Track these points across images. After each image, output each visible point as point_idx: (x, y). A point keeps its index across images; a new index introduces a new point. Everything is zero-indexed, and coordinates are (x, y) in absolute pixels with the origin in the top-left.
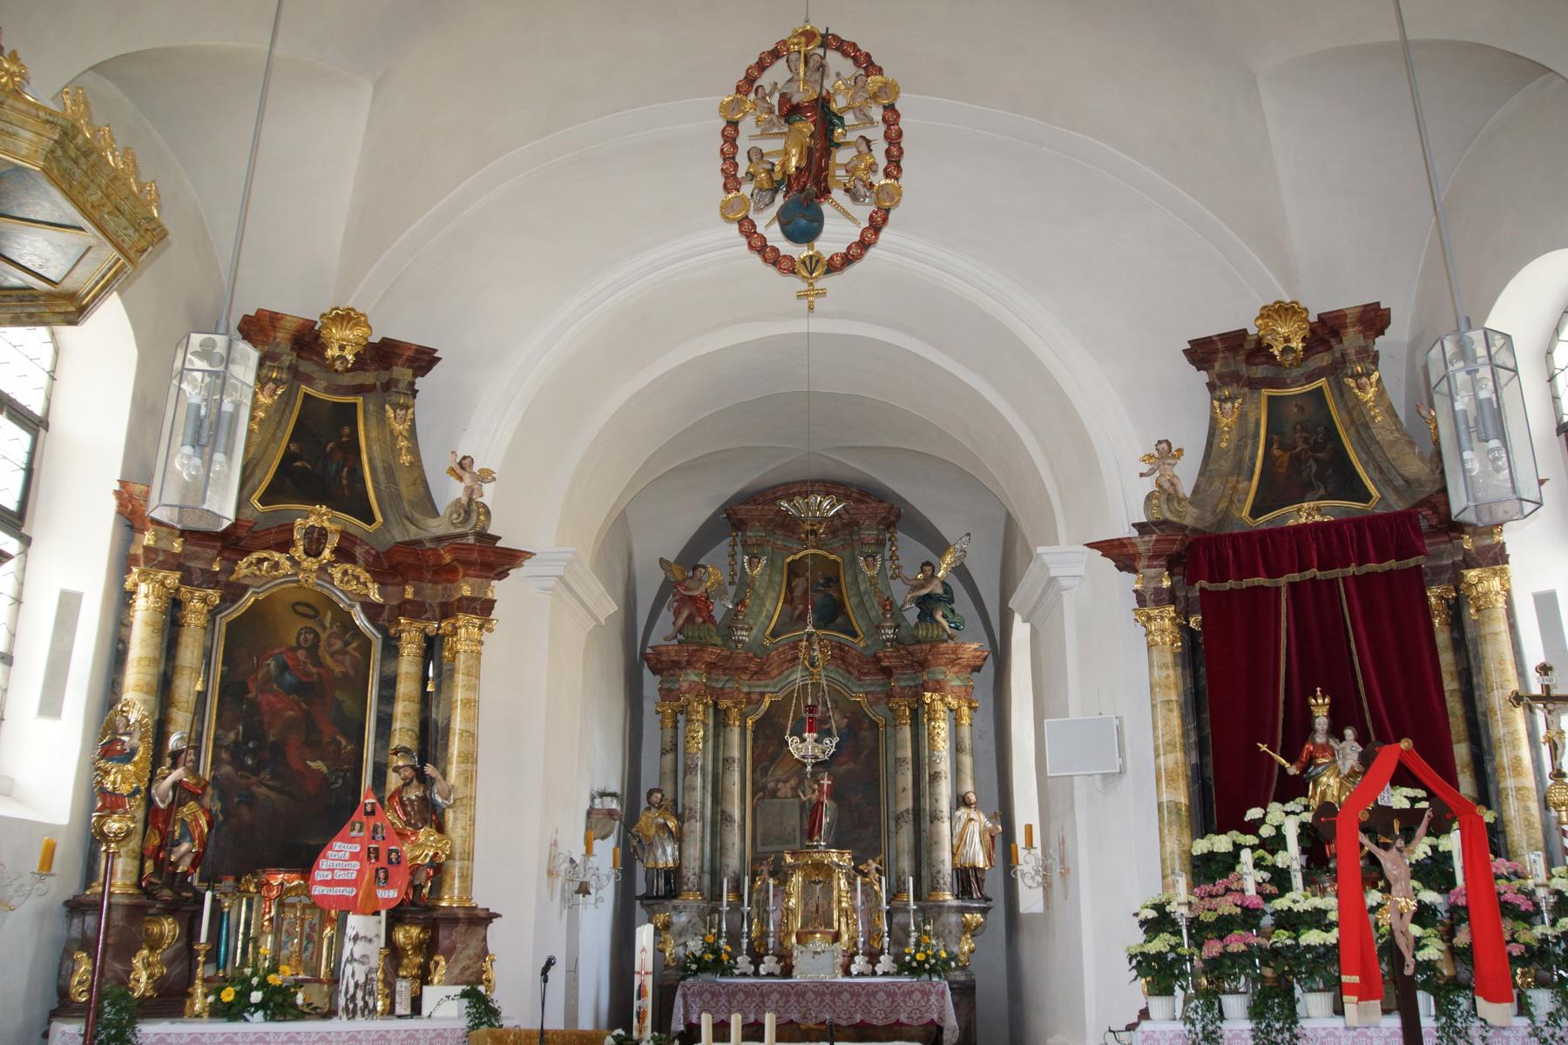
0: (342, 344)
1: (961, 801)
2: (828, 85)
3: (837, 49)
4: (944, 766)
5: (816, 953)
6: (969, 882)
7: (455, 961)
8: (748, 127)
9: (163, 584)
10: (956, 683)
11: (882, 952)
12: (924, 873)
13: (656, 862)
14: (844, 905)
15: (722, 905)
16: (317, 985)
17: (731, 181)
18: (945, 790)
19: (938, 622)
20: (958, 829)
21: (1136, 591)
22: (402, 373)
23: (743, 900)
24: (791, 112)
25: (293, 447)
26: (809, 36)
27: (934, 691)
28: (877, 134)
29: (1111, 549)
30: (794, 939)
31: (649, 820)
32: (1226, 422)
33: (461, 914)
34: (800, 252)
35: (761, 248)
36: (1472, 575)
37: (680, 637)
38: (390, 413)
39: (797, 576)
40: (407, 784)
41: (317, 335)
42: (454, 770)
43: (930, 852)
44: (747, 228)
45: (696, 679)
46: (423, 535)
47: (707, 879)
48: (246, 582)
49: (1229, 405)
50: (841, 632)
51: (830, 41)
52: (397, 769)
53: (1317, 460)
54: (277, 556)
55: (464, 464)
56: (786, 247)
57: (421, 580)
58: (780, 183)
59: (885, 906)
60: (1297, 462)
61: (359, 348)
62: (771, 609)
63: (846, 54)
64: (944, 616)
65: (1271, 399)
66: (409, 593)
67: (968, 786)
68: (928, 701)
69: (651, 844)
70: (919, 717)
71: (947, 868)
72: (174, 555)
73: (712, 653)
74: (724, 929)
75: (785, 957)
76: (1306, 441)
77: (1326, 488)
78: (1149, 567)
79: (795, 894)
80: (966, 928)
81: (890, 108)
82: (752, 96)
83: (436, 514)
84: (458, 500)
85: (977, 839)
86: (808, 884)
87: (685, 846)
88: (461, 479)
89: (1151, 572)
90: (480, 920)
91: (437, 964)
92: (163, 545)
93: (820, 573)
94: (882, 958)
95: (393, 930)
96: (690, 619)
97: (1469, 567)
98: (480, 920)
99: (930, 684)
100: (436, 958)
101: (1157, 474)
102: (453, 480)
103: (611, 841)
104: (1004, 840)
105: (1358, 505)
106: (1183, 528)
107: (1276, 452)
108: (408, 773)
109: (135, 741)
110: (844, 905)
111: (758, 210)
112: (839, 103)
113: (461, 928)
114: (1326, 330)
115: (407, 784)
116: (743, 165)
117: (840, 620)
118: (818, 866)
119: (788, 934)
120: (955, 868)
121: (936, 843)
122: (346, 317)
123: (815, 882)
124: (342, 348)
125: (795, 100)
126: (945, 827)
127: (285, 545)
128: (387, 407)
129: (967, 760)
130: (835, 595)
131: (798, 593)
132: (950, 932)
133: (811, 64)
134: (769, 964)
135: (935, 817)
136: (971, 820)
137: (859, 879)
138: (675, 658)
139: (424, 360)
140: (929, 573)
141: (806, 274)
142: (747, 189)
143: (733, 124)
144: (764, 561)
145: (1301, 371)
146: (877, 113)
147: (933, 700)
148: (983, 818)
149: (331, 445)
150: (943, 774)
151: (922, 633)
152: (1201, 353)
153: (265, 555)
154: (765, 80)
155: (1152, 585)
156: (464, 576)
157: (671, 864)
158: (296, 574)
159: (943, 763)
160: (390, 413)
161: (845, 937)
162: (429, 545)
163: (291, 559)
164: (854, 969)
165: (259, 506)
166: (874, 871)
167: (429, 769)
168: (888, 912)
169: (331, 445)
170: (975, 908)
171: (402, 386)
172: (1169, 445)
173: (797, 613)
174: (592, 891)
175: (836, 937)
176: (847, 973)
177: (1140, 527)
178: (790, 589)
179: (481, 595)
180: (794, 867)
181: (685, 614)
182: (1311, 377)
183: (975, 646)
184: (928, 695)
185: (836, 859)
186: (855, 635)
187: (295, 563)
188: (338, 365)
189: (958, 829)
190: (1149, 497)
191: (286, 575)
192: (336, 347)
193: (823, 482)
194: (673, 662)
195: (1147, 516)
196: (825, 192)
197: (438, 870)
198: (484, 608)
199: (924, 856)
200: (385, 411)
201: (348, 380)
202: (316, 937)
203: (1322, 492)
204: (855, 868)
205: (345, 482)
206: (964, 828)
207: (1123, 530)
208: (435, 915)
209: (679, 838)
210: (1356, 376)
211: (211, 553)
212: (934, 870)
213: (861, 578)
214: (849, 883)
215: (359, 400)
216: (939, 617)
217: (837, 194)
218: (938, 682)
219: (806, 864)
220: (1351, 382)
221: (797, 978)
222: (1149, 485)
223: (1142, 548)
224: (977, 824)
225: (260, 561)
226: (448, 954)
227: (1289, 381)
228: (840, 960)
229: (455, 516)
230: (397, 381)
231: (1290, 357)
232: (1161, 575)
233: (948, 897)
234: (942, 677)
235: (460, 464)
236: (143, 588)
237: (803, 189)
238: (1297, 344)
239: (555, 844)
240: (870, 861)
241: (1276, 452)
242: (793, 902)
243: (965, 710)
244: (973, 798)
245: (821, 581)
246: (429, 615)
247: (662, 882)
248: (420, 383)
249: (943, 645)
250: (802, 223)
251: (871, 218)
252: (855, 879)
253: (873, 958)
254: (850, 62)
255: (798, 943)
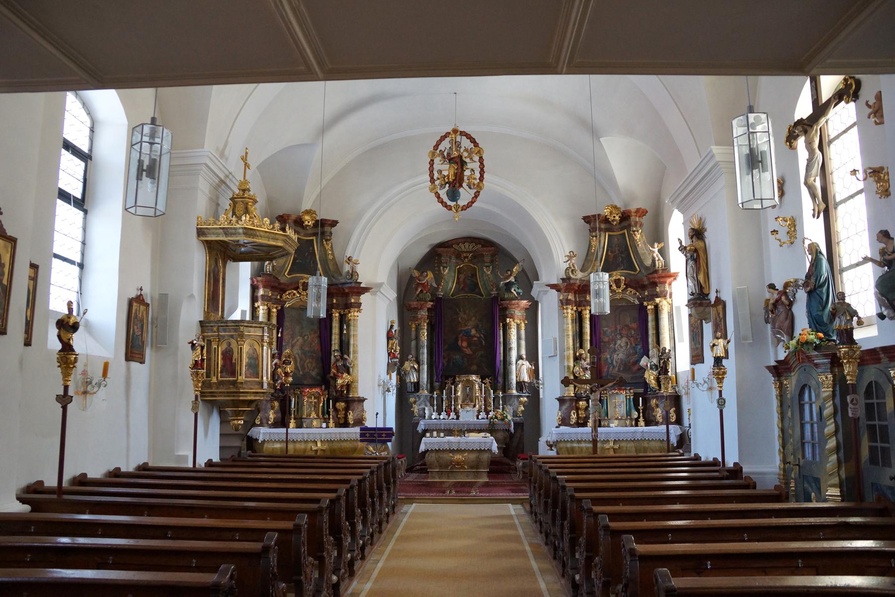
0: (308, 221)
1: (520, 357)
2: (462, 150)
3: (465, 136)
4: (514, 345)
5: (468, 411)
6: (523, 387)
7: (355, 412)
8: (437, 160)
9: (267, 306)
10: (520, 314)
11: (491, 411)
12: (506, 383)
13: (410, 379)
14: (477, 394)
15: (434, 394)
16: (319, 420)
17: (432, 180)
18: (514, 354)
19: (512, 292)
20: (519, 367)
21: (560, 300)
22: (327, 229)
23: (443, 394)
24: (451, 160)
25: (296, 256)
26: (455, 131)
27: (511, 318)
28: (476, 166)
29: (553, 286)
30: (460, 407)
31: (407, 365)
32: (593, 243)
33: (356, 399)
34: (452, 204)
35: (442, 202)
36: (658, 300)
37: (418, 298)
38: (325, 243)
39: (461, 273)
40: (337, 360)
41: (301, 219)
42: (351, 356)
43: (508, 376)
44: (438, 196)
45: (424, 314)
46: (337, 282)
47: (429, 385)
48: (286, 300)
49: (595, 238)
50: (477, 294)
51: (463, 134)
52: (335, 356)
53: (622, 257)
54: (295, 292)
55: (349, 259)
56: (449, 203)
57: (338, 297)
58: (447, 183)
59: (492, 396)
60: (615, 257)
61: (313, 222)
62: (451, 286)
63: (467, 138)
64: (515, 290)
65: (609, 235)
66: (335, 301)
67: (523, 352)
68: (508, 322)
69: (409, 373)
70: (506, 328)
71: (514, 382)
72: (270, 297)
73: (430, 304)
74: (435, 403)
75: (457, 413)
76: (619, 250)
77: (624, 267)
78: (565, 292)
79: (460, 391)
80: (521, 403)
81: (481, 160)
82: (438, 151)
83: (341, 274)
84: (348, 272)
85: (525, 371)
86: (464, 388)
87: (420, 375)
88: (349, 264)
89: (566, 294)
90: (362, 400)
91: (350, 413)
92: (266, 294)
93: (469, 272)
94: (490, 413)
95: (336, 404)
96: (421, 291)
97: (658, 297)
98: (362, 400)
99: (509, 315)
100: (350, 412)
101: (569, 262)
102: (347, 264)
103: (395, 373)
104: (535, 373)
105: (632, 273)
106: (576, 279)
107: (609, 253)
108: (339, 357)
109: (291, 360)
110: (477, 394)
111: (440, 189)
112: (465, 154)
113: (356, 403)
114: (625, 217)
115: (337, 360)
116: (436, 175)
117: (477, 290)
118: (468, 381)
119: (458, 405)
120: (517, 383)
121: (510, 373)
122: (308, 212)
123: (467, 387)
124: (309, 222)
125: (452, 156)
126: (514, 367)
127: (297, 288)
128: (324, 240)
129: (523, 343)
130: (475, 281)
131: (461, 280)
132: (515, 404)
133: (457, 144)
134: (453, 415)
135: (510, 364)
136: (523, 364)
137: (483, 385)
138: (416, 306)
139: (334, 223)
140: (509, 274)
141: (455, 211)
142: (437, 183)
143: (432, 160)
144: (448, 267)
145: (619, 227)
146: (476, 158)
147: (510, 321)
148: (528, 363)
149: (307, 254)
150: (513, 349)
151: (506, 296)
152: (587, 219)
153: (290, 292)
154: (441, 147)
155: (566, 298)
156: (352, 296)
157: (416, 381)
158: (300, 296)
159: (513, 344)
160: (325, 243)
161: (477, 406)
162: (340, 286)
163: (298, 292)
164: (480, 417)
165: (287, 276)
166: (488, 382)
167: (346, 356)
168: (494, 398)
169: (307, 254)
170: (524, 396)
171: (328, 234)
172: (573, 252)
173: (461, 288)
174: (391, 391)
175: (474, 406)
176: (478, 418)
177: (563, 279)
178: (458, 278)
179: (357, 301)
180: (459, 381)
181: (420, 290)
182: (622, 229)
183: (526, 301)
184: (508, 319)
185: (474, 379)
186: (482, 296)
187: (300, 294)
188: (308, 228)
189: (519, 367)
190: (567, 269)
191: (297, 297)
192: (307, 222)
193: (470, 238)
194: (415, 308)
195: (566, 275)
196: (461, 186)
197: (348, 386)
198: (358, 305)
199: (506, 377)
200: (323, 242)
201: (310, 231)
202: (317, 406)
203: (622, 268)
204: (482, 382)
205: (312, 265)
206: (520, 367)
207: (554, 282)
208: (349, 399)
209: (418, 371)
210: (634, 231)
211: (276, 293)
212: (509, 382)
213: (484, 275)
214: (479, 387)
215: (314, 238)
216: (513, 291)
217: (464, 185)
218: (512, 314)
219: (464, 380)
220: (631, 232)
221: (461, 419)
222: (566, 265)
223: (562, 287)
224: (526, 365)
225: (289, 294)
226: (353, 411)
227: (615, 230)
228: (476, 414)
229: (348, 276)
230: (326, 232)
231: (615, 223)
232: (569, 295)
233: (514, 392)
234: (513, 313)
235: (349, 259)
236: (261, 307)
237: (454, 186)
238: (617, 218)
239: (380, 376)
240: (487, 379)
241: (609, 253)
242: (459, 394)
243: (523, 325)
244: (524, 356)
245: (470, 275)
246: (340, 308)
247: (413, 386)
248: (333, 229)
249: (514, 302)
250: (454, 195)
251: (475, 194)
252: (482, 385)
253: (487, 413)
254: (469, 140)
255: (461, 407)
